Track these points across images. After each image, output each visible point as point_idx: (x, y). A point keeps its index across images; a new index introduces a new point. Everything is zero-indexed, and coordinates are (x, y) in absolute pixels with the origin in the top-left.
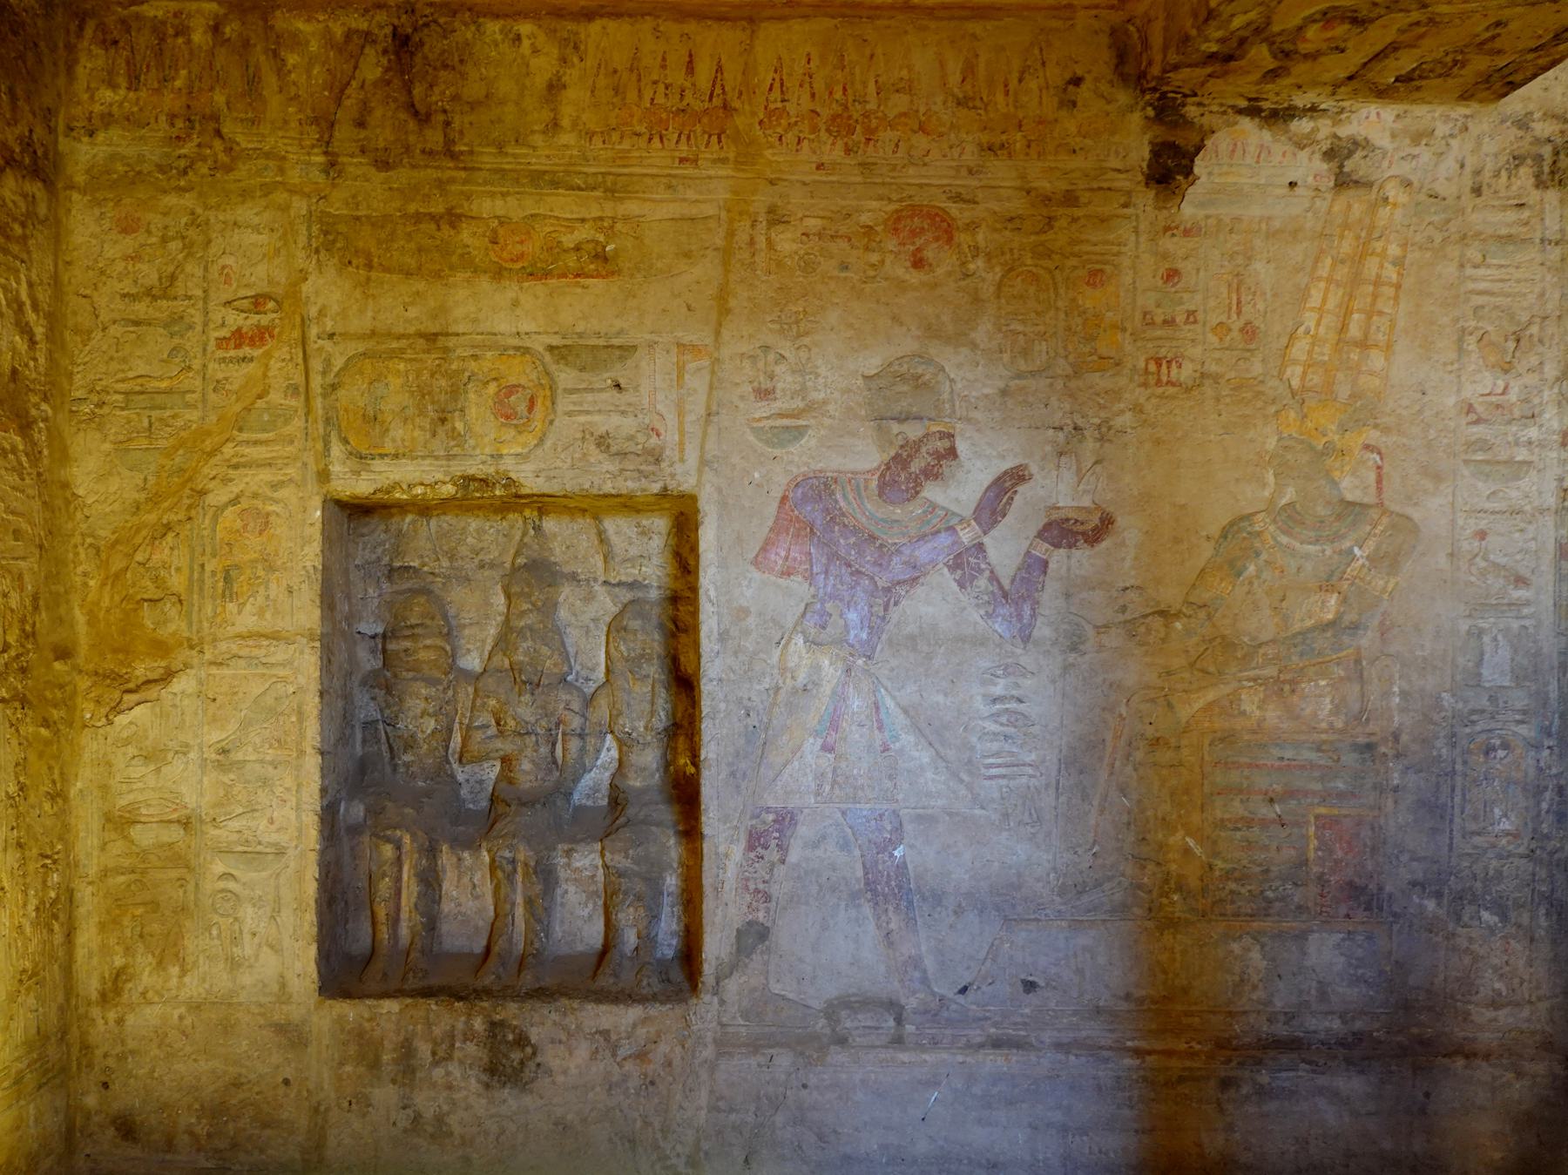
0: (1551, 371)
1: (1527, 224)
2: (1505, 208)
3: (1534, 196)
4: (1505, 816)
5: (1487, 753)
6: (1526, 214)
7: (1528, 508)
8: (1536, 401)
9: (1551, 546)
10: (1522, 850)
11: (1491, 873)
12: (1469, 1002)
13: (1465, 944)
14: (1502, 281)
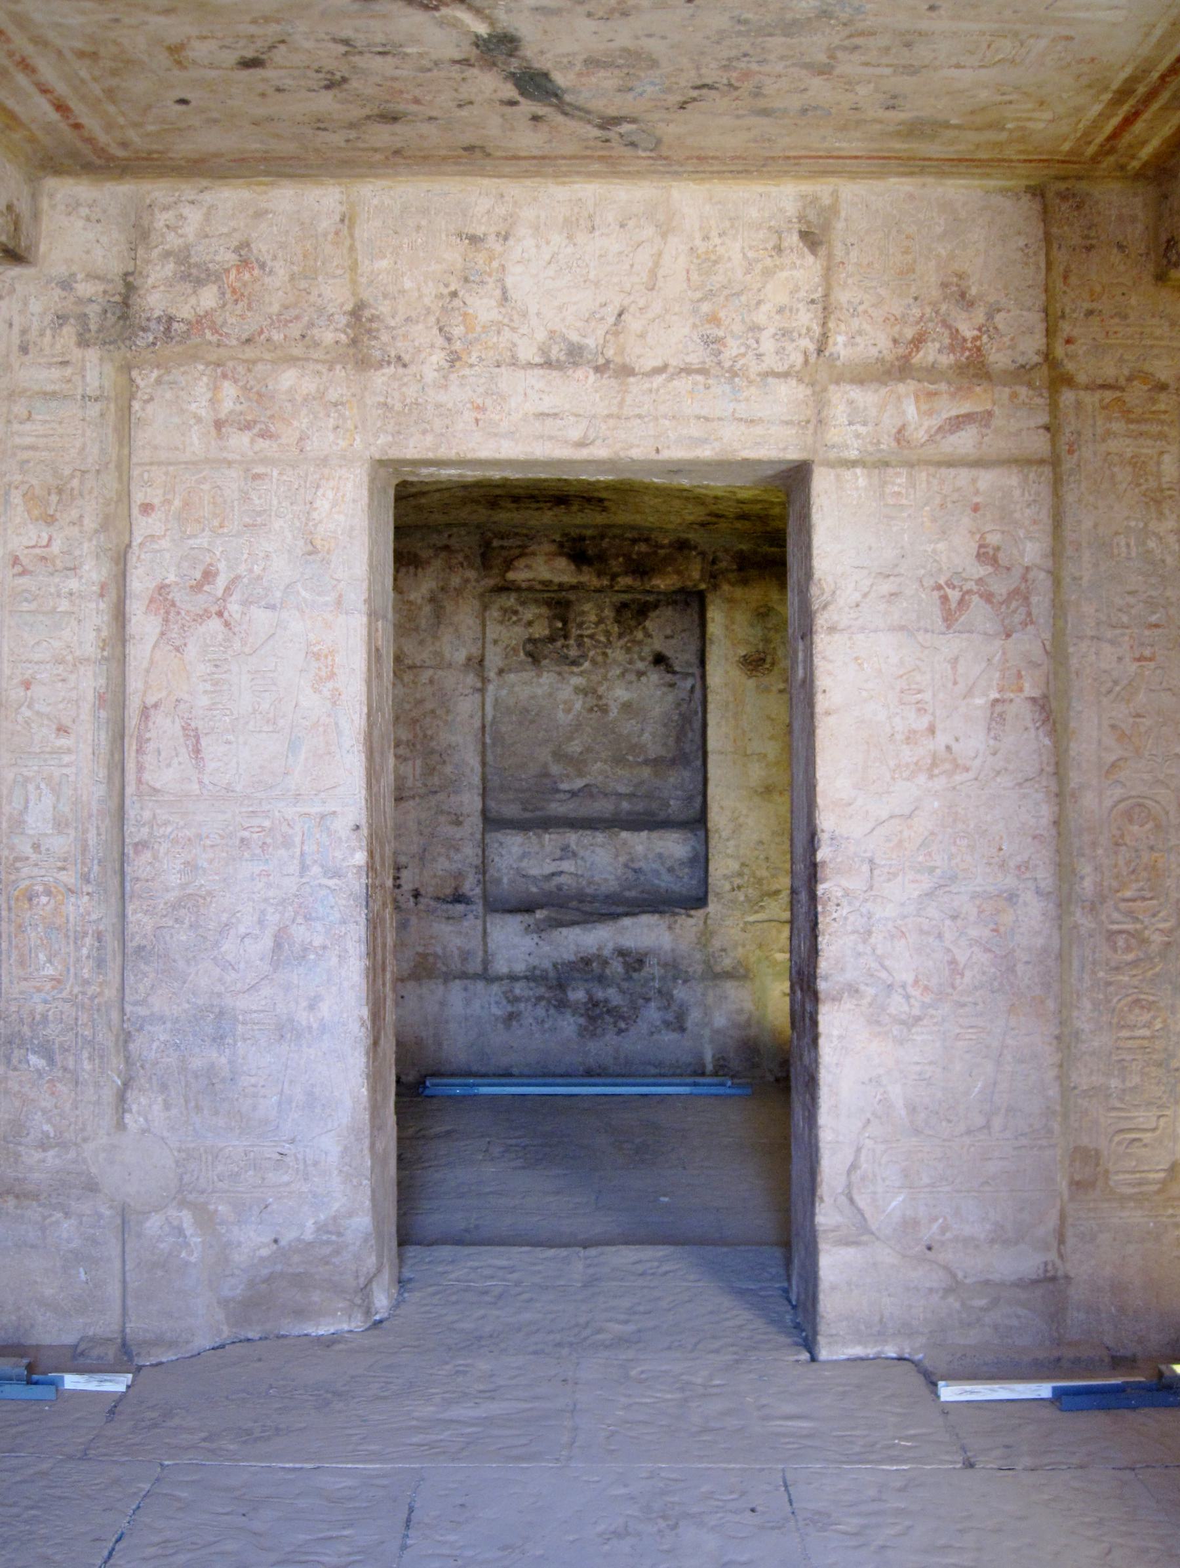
0: (90, 524)
1: (69, 381)
2: (50, 365)
3: (76, 353)
4: (50, 961)
5: (30, 900)
6: (69, 371)
7: (70, 658)
8: (77, 553)
9: (90, 696)
10: (64, 994)
11: (38, 1017)
12: (20, 1144)
13: (17, 1088)
14: (45, 436)
